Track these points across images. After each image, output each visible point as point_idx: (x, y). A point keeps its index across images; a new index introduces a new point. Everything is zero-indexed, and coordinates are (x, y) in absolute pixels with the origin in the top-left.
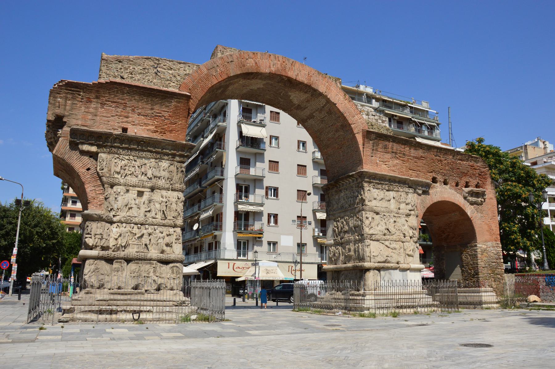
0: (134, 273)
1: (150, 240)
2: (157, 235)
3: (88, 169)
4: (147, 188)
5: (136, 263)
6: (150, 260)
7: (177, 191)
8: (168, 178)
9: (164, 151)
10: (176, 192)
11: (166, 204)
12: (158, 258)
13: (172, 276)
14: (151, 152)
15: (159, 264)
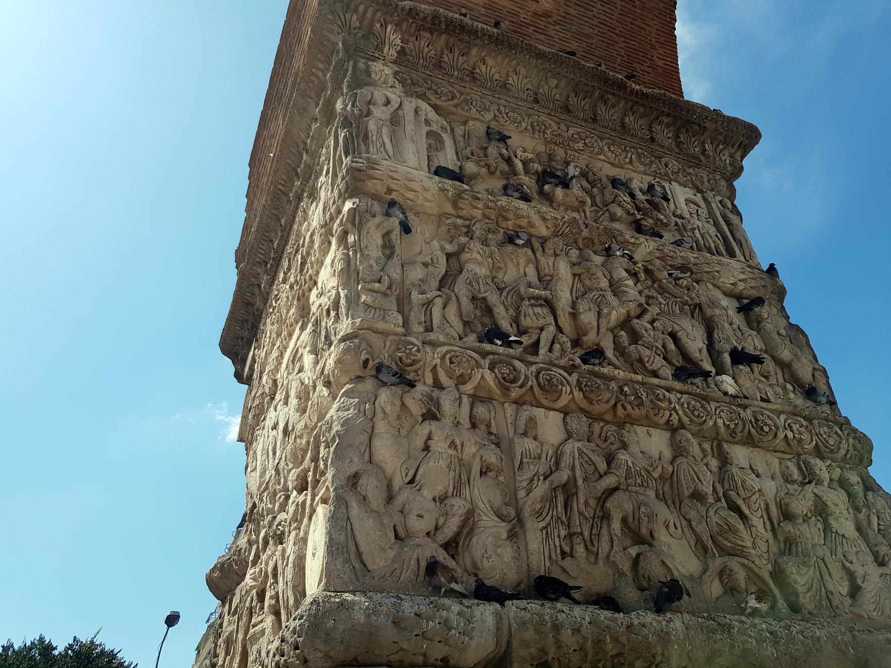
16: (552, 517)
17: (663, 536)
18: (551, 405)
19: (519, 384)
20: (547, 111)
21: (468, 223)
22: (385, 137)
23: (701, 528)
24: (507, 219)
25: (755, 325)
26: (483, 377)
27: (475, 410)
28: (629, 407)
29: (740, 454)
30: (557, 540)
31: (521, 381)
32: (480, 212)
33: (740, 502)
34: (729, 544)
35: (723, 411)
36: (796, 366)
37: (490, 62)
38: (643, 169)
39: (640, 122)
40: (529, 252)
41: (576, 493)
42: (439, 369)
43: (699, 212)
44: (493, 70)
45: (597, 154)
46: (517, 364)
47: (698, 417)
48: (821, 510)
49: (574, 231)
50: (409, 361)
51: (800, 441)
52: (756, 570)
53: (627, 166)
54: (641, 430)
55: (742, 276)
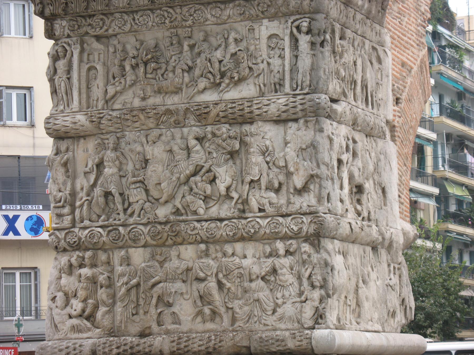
16: (129, 301)
18: (138, 245)
19: (120, 240)
26: (104, 241)
28: (174, 238)
30: (130, 310)
31: (121, 239)
34: (208, 300)
35: (228, 226)
36: (295, 177)
38: (240, 19)
43: (279, 44)
45: (204, 22)
46: (121, 228)
47: (212, 234)
49: (170, 116)
50: (72, 243)
52: (217, 311)
53: (229, 21)
54: (182, 248)
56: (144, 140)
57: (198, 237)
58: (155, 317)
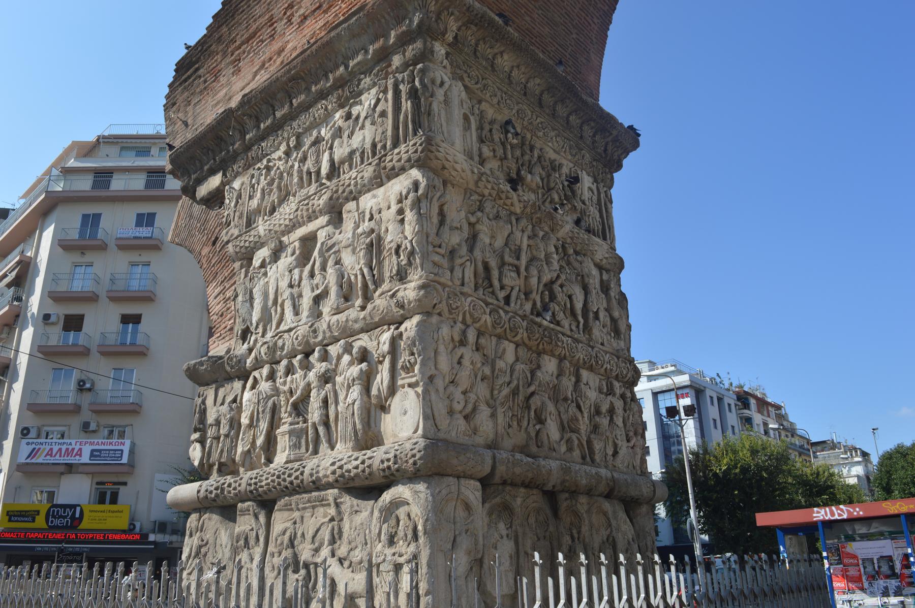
0: (280, 553)
1: (325, 402)
2: (343, 376)
3: (214, 243)
4: (322, 213)
5: (288, 508)
6: (318, 489)
7: (403, 170)
8: (374, 145)
9: (352, 64)
10: (401, 177)
11: (368, 240)
12: (334, 473)
13: (389, 551)
14: (323, 95)
15: (348, 501)
17: (549, 421)
20: (529, 103)
21: (480, 198)
22: (442, 119)
23: (564, 417)
24: (501, 199)
25: (605, 289)
27: (480, 341)
28: (545, 344)
29: (584, 374)
32: (488, 191)
33: (582, 404)
37: (506, 57)
39: (578, 121)
40: (510, 226)
41: (518, 394)
42: (467, 313)
44: (505, 64)
48: (611, 411)
51: (611, 370)
55: (607, 256)
56: (514, 221)
57: (564, 351)
58: (533, 434)
